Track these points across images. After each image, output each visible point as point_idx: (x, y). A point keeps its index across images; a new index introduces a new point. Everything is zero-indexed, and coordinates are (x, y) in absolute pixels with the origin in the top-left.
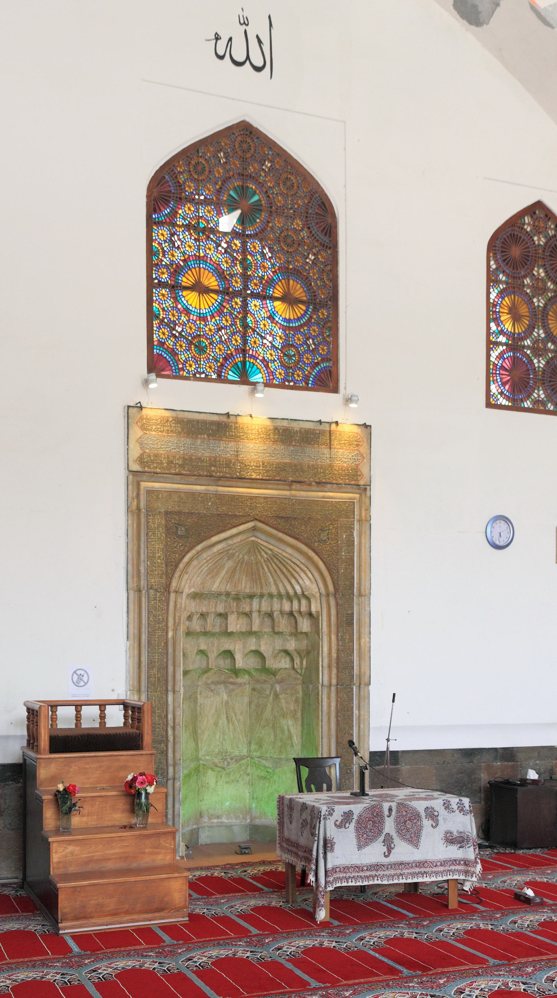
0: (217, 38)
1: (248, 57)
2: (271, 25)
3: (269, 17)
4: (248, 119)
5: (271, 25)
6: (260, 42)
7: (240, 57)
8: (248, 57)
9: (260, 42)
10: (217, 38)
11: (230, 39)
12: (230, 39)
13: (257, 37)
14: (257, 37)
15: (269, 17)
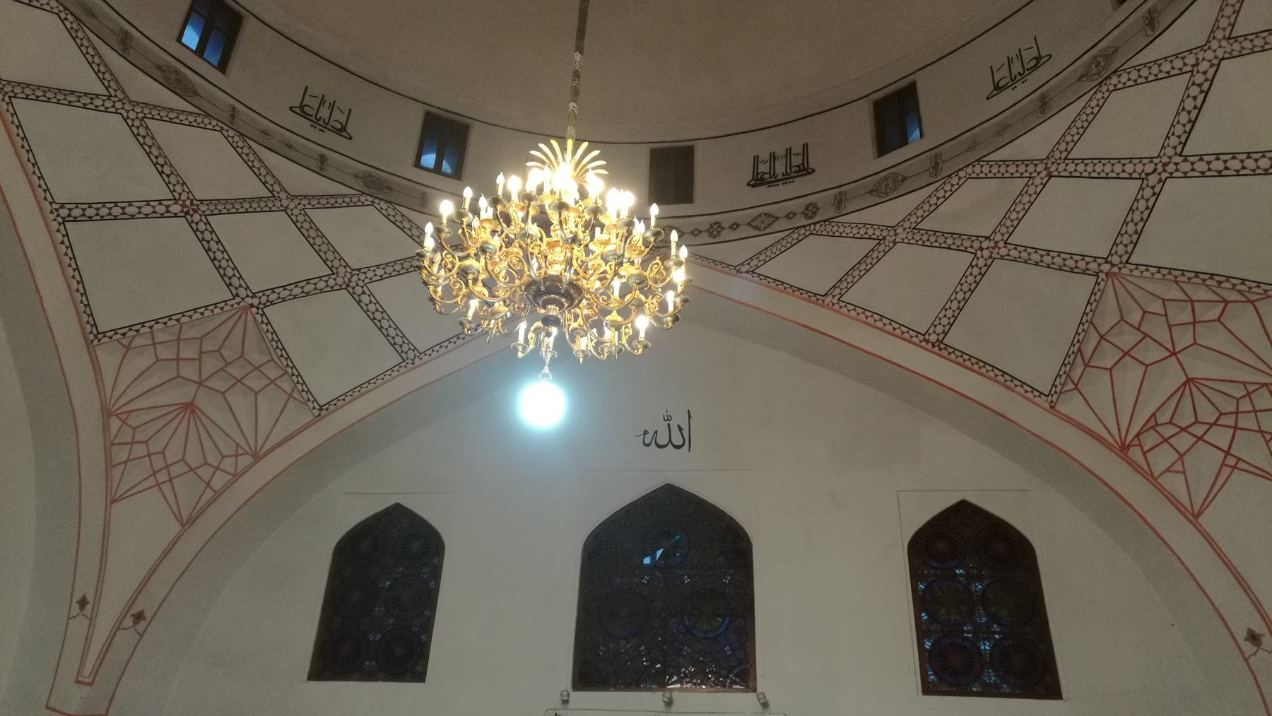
0: (646, 433)
1: (670, 441)
2: (690, 416)
3: (689, 411)
4: (670, 482)
5: (690, 416)
6: (680, 428)
7: (663, 440)
8: (670, 441)
9: (680, 428)
10: (646, 433)
11: (656, 432)
12: (656, 432)
13: (679, 426)
14: (679, 426)
15: (689, 411)
